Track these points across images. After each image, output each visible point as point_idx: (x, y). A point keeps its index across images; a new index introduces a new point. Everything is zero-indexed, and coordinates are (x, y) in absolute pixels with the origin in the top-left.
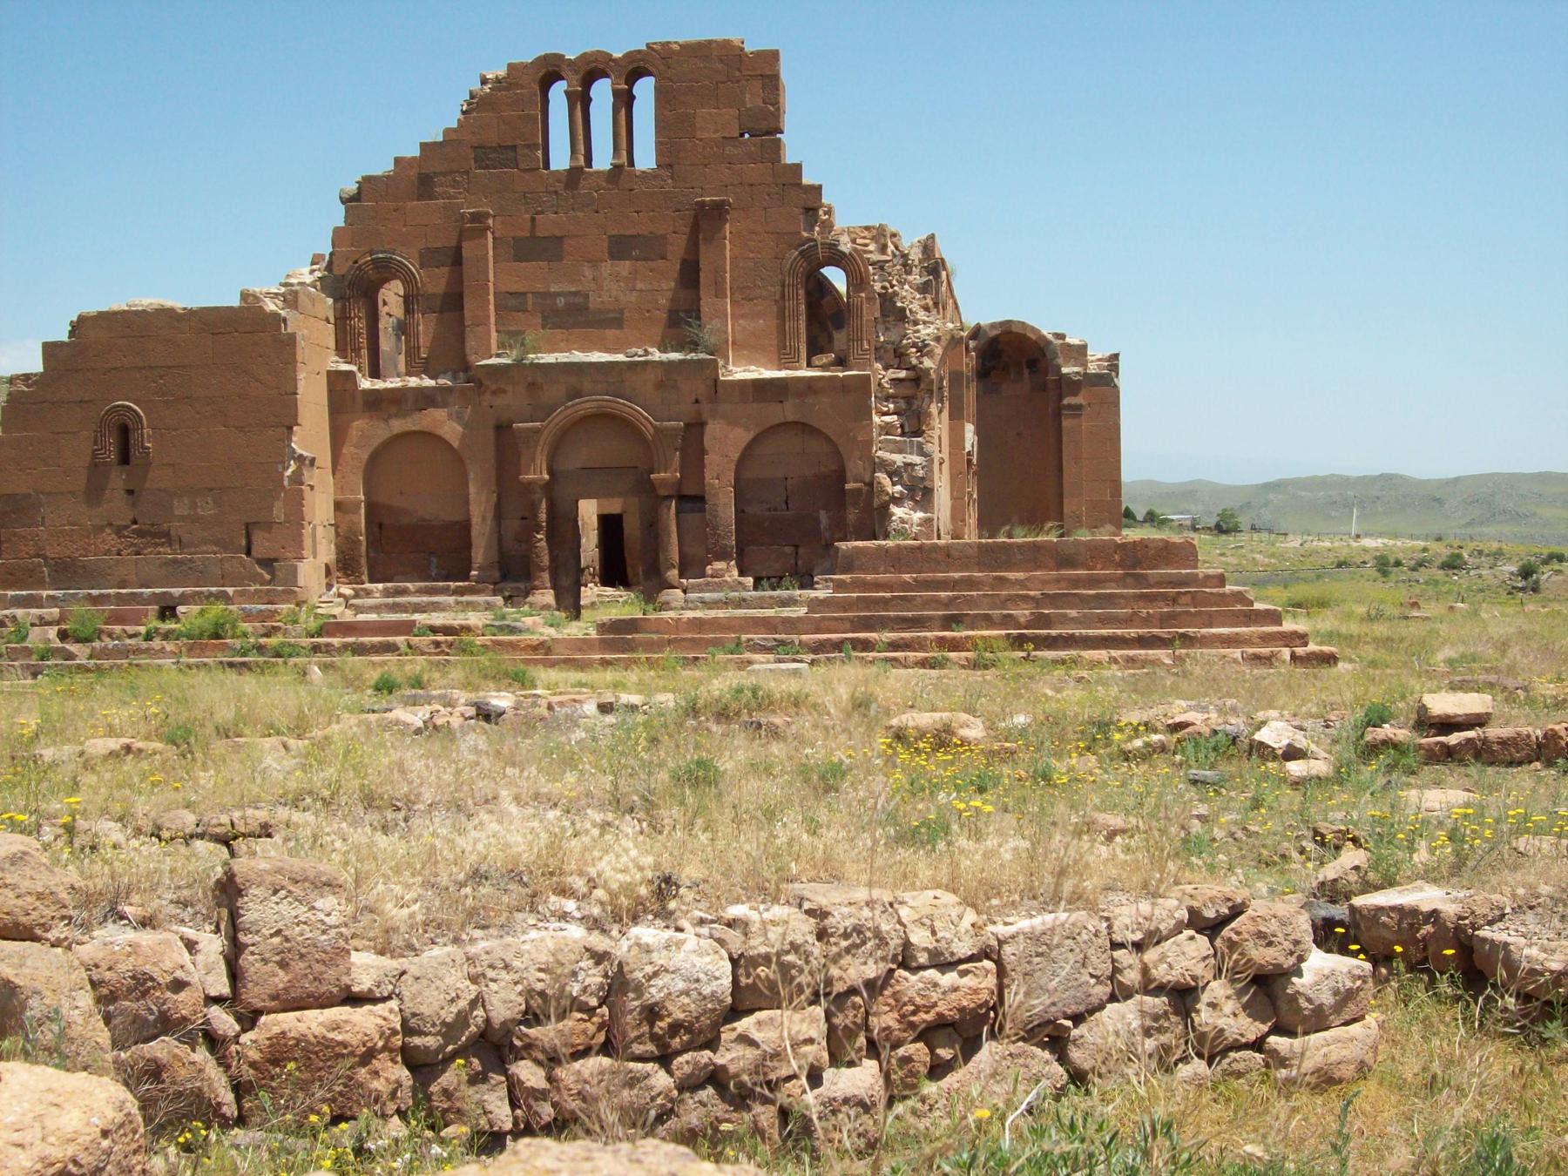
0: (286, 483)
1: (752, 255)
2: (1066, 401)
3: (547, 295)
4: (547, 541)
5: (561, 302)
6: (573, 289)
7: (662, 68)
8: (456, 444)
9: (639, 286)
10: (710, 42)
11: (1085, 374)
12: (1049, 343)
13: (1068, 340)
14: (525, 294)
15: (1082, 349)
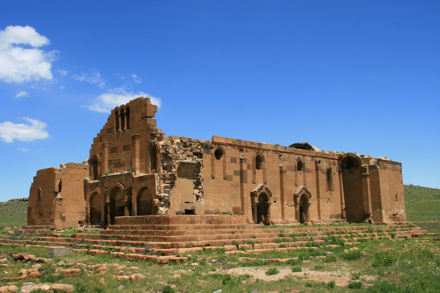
0: (54, 204)
1: (143, 147)
2: (363, 174)
3: (115, 160)
4: (110, 216)
5: (117, 161)
6: (118, 158)
7: (131, 106)
8: (100, 194)
9: (127, 156)
10: (137, 98)
11: (369, 166)
12: (359, 158)
13: (365, 157)
14: (112, 160)
15: (368, 159)
